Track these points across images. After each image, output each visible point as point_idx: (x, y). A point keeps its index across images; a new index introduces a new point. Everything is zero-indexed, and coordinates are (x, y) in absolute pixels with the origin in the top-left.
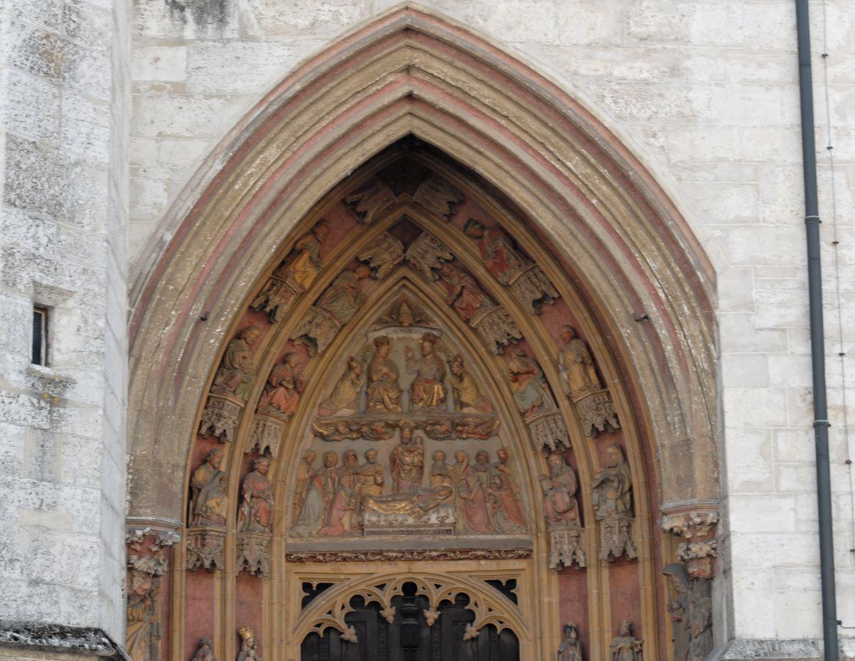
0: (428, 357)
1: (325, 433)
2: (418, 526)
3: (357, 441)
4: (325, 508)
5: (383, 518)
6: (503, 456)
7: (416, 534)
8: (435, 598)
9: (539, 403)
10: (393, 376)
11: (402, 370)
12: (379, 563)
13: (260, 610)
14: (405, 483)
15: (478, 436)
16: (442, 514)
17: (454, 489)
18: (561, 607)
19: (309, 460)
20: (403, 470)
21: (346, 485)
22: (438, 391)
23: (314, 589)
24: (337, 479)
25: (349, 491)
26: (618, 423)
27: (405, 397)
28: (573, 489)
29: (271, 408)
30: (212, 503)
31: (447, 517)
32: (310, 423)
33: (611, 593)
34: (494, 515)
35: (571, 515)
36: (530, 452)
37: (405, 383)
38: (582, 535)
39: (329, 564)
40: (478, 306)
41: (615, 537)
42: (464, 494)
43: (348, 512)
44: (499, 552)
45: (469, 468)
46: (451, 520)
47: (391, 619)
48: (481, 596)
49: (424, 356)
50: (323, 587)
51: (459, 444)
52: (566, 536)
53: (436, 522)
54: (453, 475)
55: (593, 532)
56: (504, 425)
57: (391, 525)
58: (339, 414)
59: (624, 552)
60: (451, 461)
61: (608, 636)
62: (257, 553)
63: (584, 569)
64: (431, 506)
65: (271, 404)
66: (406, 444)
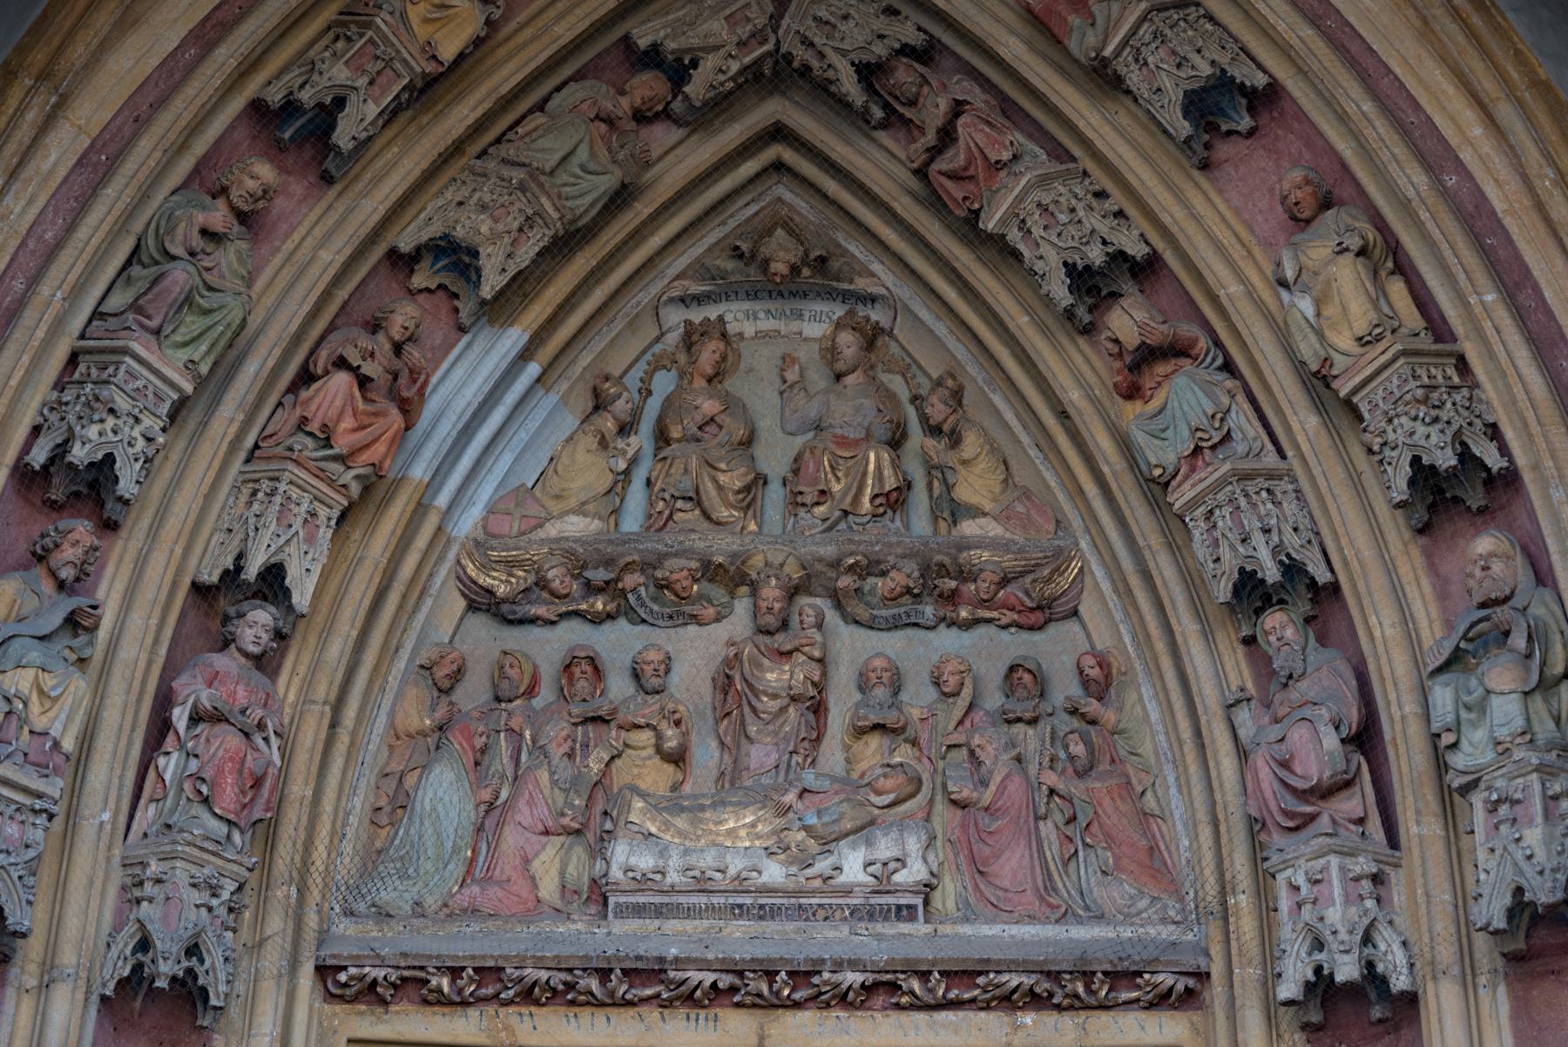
0: (850, 380)
1: (502, 590)
2: (798, 893)
3: (607, 627)
4: (480, 829)
5: (675, 862)
6: (1095, 673)
7: (789, 918)
11: (767, 423)
12: (652, 1014)
14: (761, 755)
16: (885, 848)
17: (925, 777)
19: (440, 673)
20: (754, 710)
22: (879, 467)
24: (527, 734)
25: (566, 771)
26: (1504, 450)
27: (774, 496)
28: (1353, 716)
31: (901, 861)
32: (451, 555)
34: (1066, 863)
35: (1349, 804)
36: (1186, 626)
37: (774, 457)
39: (473, 1013)
40: (1006, 156)
41: (1534, 836)
43: (558, 840)
44: (1088, 976)
45: (978, 716)
46: (914, 873)
49: (839, 377)
51: (947, 641)
52: (1335, 874)
54: (924, 737)
55: (1437, 850)
57: (702, 884)
58: (552, 530)
60: (918, 699)
62: (192, 915)
63: (1411, 1000)
65: (302, 425)
66: (769, 633)
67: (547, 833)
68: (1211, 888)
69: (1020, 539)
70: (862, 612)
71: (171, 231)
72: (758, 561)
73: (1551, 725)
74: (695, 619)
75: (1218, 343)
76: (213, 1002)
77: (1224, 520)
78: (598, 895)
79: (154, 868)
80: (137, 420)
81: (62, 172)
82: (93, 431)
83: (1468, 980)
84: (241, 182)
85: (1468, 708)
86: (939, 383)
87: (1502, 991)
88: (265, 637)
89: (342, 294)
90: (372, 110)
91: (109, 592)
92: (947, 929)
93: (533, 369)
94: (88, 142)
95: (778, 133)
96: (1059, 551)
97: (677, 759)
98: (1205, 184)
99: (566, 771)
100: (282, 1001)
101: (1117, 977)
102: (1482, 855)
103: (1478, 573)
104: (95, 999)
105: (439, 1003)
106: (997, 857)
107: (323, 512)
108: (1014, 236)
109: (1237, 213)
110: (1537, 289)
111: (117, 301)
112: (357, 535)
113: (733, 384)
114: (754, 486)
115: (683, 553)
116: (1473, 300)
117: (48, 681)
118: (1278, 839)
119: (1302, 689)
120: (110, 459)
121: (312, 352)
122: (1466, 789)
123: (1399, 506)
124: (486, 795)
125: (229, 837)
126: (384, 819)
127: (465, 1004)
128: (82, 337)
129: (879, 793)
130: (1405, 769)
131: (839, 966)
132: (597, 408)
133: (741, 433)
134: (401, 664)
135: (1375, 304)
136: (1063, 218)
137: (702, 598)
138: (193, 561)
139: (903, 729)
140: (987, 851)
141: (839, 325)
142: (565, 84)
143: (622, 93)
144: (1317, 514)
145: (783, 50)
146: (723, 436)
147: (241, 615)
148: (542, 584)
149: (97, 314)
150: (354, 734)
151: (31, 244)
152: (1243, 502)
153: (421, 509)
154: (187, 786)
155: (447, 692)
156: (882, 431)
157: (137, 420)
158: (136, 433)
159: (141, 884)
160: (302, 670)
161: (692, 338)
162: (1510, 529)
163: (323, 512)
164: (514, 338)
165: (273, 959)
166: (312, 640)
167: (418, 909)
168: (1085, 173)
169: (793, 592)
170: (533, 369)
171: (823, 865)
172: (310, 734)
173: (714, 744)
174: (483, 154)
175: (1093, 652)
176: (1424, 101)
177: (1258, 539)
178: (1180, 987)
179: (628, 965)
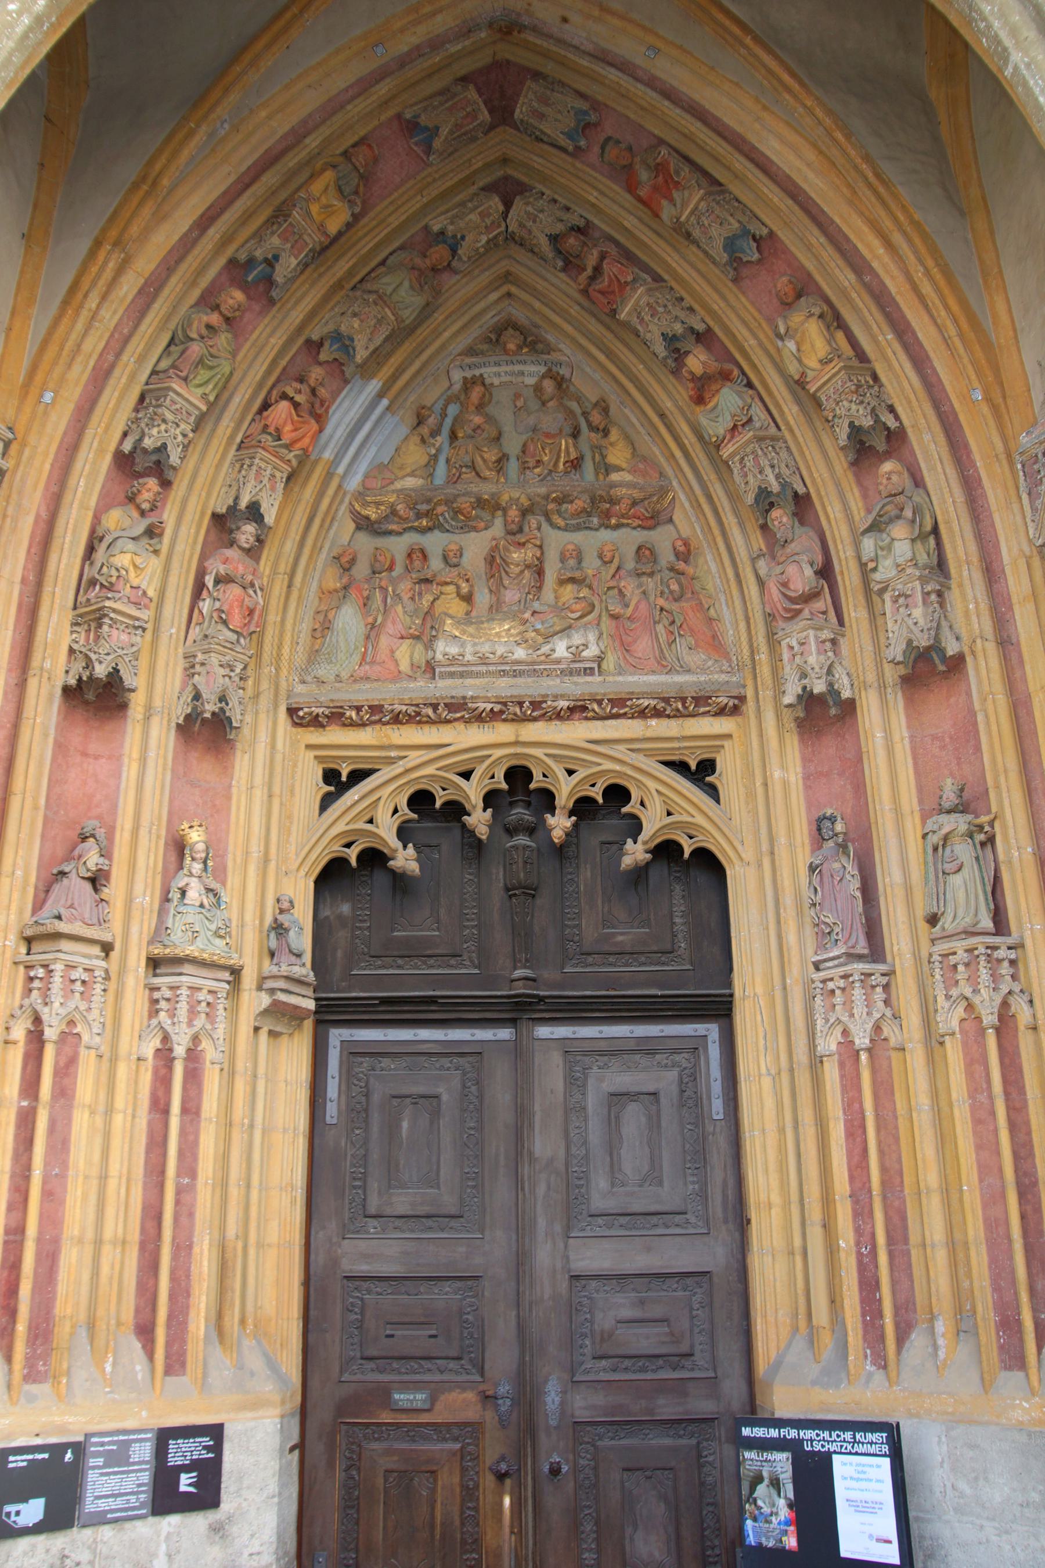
0: (551, 404)
1: (373, 517)
2: (533, 663)
3: (429, 535)
4: (368, 637)
5: (469, 649)
6: (682, 549)
8: (565, 791)
9: (745, 419)
10: (491, 431)
11: (508, 428)
12: (460, 726)
13: (229, 798)
14: (511, 595)
15: (638, 522)
17: (596, 603)
18: (807, 787)
20: (507, 573)
21: (406, 597)
22: (567, 448)
23: (344, 778)
26: (897, 418)
28: (819, 559)
29: (264, 437)
30: (123, 560)
31: (586, 646)
32: (347, 500)
33: (912, 738)
34: (670, 645)
35: (819, 605)
36: (730, 520)
37: (512, 445)
38: (842, 641)
39: (369, 729)
40: (630, 278)
41: (918, 612)
42: (616, 608)
44: (684, 700)
45: (622, 572)
46: (592, 651)
47: (483, 832)
48: (652, 785)
49: (544, 404)
50: (358, 776)
51: (605, 535)
52: (812, 639)
53: (566, 654)
54: (595, 585)
55: (865, 625)
56: (682, 496)
57: (483, 661)
58: (398, 485)
59: (937, 638)
60: (591, 565)
61: (913, 828)
62: (221, 680)
64: (558, 628)
66: (514, 534)
67: (402, 638)
68: (746, 652)
69: (641, 481)
70: (561, 523)
71: (190, 325)
72: (505, 497)
73: (925, 556)
74: (475, 529)
75: (744, 373)
76: (235, 724)
77: (749, 462)
78: (430, 669)
79: (200, 657)
80: (178, 425)
81: (130, 297)
82: (155, 431)
83: (882, 687)
84: (226, 302)
85: (882, 549)
86: (596, 405)
87: (900, 694)
88: (252, 539)
89: (283, 363)
90: (294, 262)
91: (169, 516)
92: (610, 679)
93: (385, 402)
94: (143, 281)
95: (507, 277)
96: (662, 487)
97: (468, 598)
98: (735, 289)
99: (410, 607)
100: (270, 724)
101: (698, 700)
102: (890, 624)
103: (884, 481)
104: (174, 725)
105: (351, 725)
106: (635, 641)
107: (278, 474)
108: (635, 321)
109: (752, 303)
110: (914, 333)
111: (164, 364)
112: (296, 489)
113: (490, 409)
114: (502, 460)
115: (467, 494)
116: (880, 338)
117: (138, 561)
118: (781, 624)
119: (792, 547)
120: (164, 446)
121: (269, 392)
122: (882, 592)
123: (842, 449)
124: (370, 620)
125: (238, 641)
126: (318, 634)
127: (364, 725)
128: (147, 384)
129: (573, 612)
130: (847, 583)
131: (556, 697)
132: (418, 424)
133: (494, 434)
134: (323, 555)
135: (829, 343)
136: (661, 310)
137: (477, 517)
138: (212, 502)
139: (584, 580)
140: (630, 639)
141: (543, 377)
142: (394, 251)
143: (425, 256)
144: (798, 459)
145: (510, 230)
146: (485, 435)
147: (238, 528)
148: (394, 512)
149: (154, 372)
150: (300, 590)
151: (116, 336)
152: (760, 453)
153: (329, 475)
154: (215, 615)
155: (348, 570)
156: (568, 430)
157: (178, 425)
158: (178, 431)
159: (193, 667)
160: (272, 558)
161: (468, 384)
162: (900, 460)
163: (278, 474)
164: (374, 386)
165: (265, 701)
166: (276, 543)
167: (338, 678)
168: (672, 289)
169: (524, 513)
170: (385, 402)
171: (545, 649)
172: (278, 589)
173: (487, 591)
174: (354, 288)
175: (680, 538)
176: (852, 237)
177: (768, 471)
178: (731, 704)
179: (447, 701)
